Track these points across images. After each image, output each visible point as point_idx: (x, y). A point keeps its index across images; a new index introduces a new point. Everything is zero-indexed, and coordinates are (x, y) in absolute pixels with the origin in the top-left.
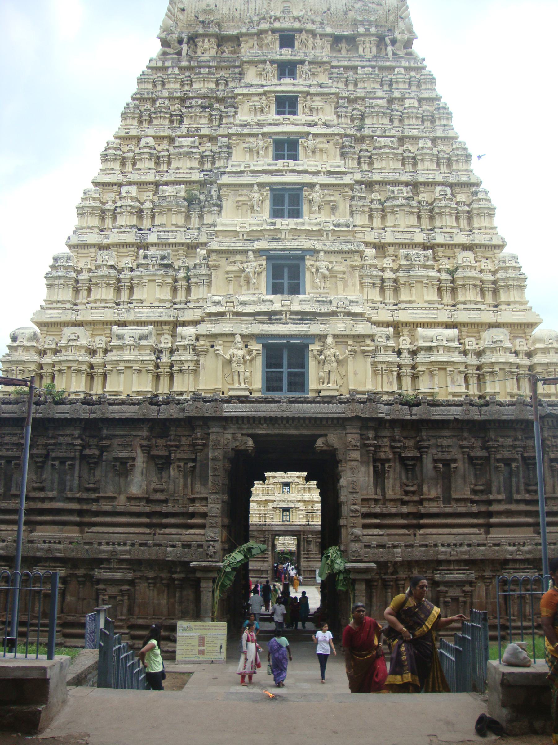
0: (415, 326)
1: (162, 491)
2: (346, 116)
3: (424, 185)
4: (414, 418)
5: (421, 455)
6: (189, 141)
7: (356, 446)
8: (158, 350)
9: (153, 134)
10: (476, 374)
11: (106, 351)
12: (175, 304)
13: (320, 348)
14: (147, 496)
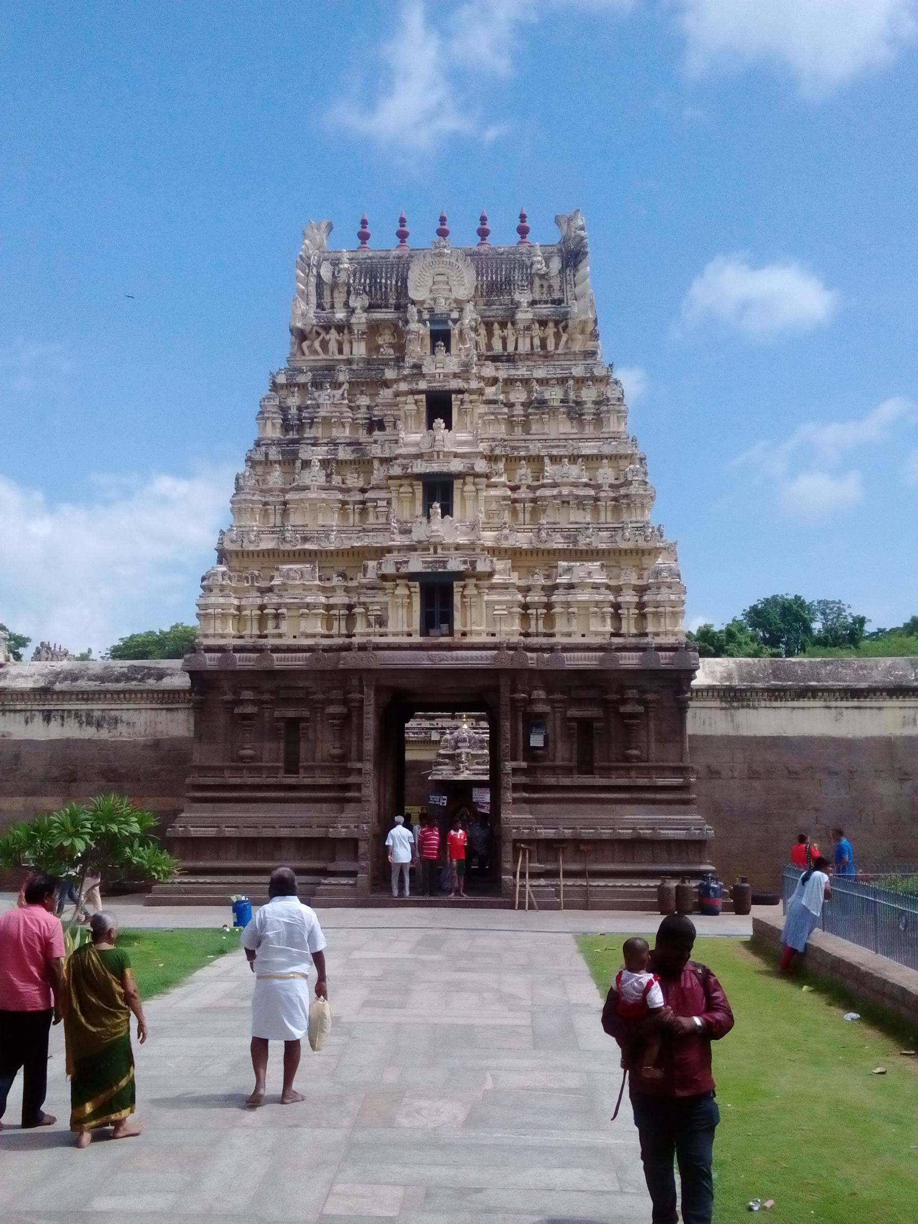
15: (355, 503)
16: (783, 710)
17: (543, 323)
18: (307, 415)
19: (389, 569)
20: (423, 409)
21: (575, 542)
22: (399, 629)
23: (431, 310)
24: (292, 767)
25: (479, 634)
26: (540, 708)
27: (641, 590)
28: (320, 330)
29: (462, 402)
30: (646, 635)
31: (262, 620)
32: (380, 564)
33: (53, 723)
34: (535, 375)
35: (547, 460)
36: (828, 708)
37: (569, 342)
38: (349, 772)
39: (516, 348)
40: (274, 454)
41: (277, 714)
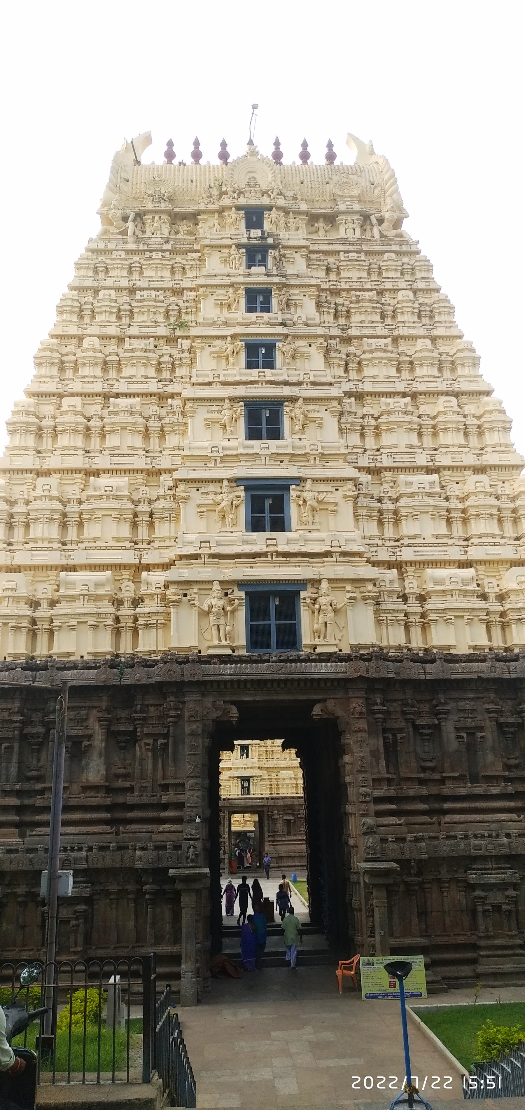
0: (422, 565)
1: (126, 776)
2: (328, 312)
3: (425, 395)
4: (428, 677)
5: (440, 723)
6: (142, 343)
7: (361, 713)
8: (117, 599)
9: (98, 333)
10: (499, 622)
11: (53, 603)
12: (136, 543)
13: (313, 595)
14: (108, 784)
26: (276, 816)
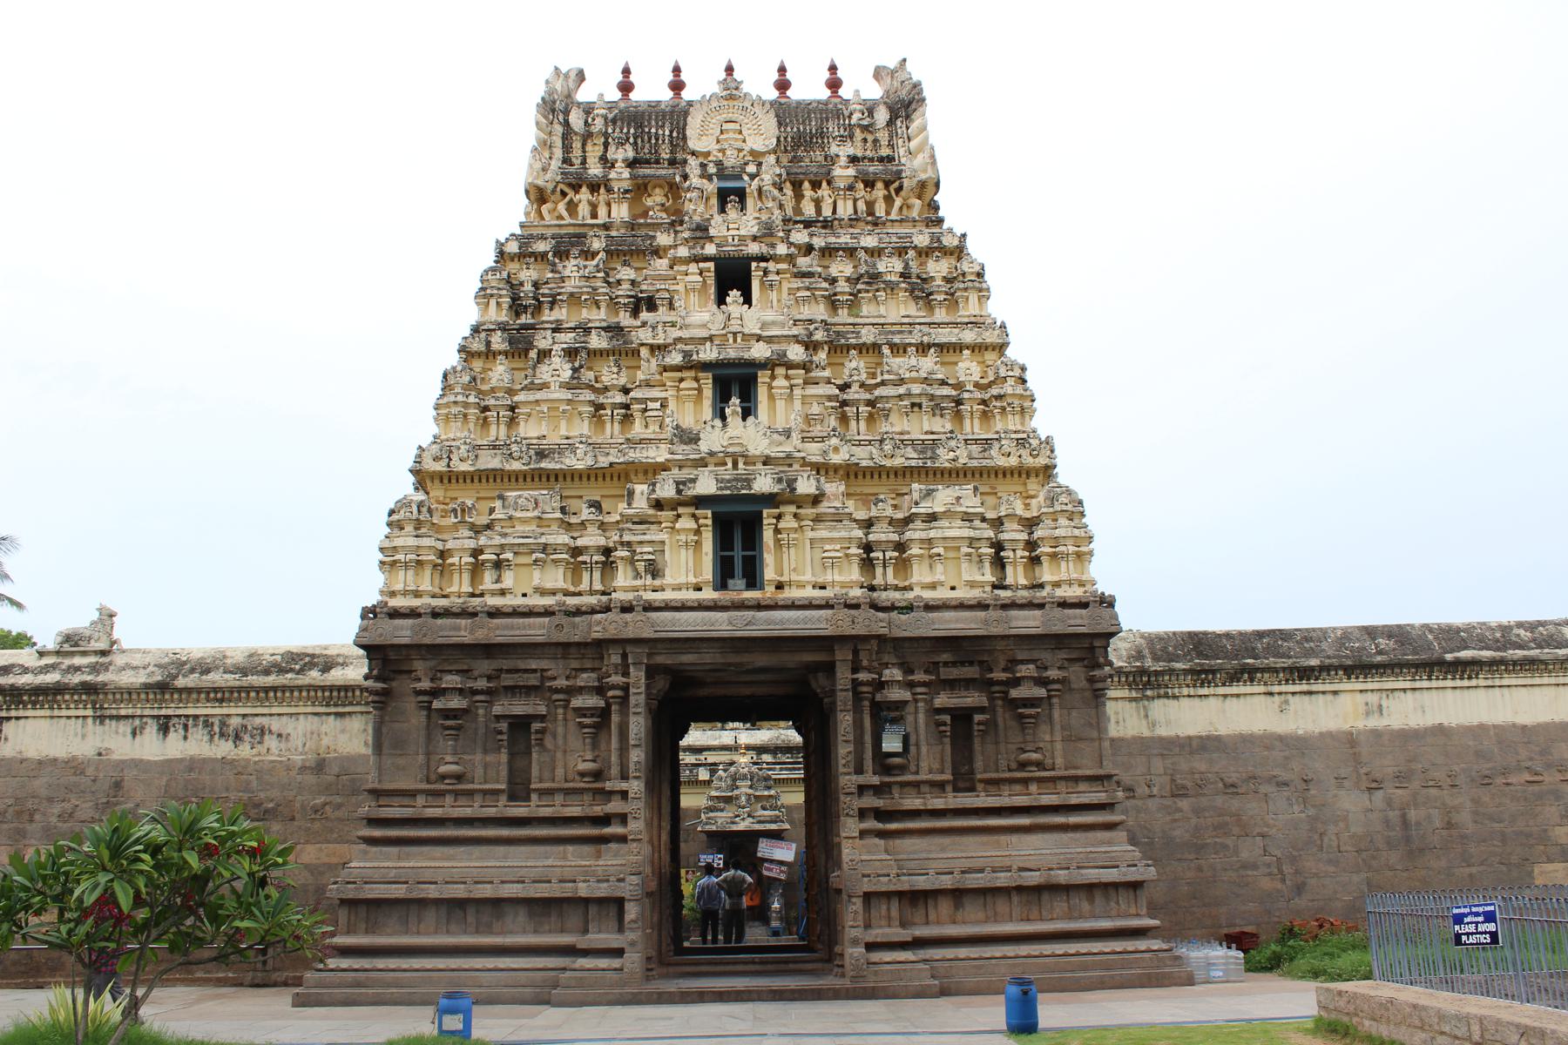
15: (615, 406)
16: (1211, 698)
17: (870, 184)
18: (547, 291)
19: (667, 491)
20: (711, 282)
21: (934, 458)
22: (682, 580)
23: (719, 164)
24: (519, 790)
25: (801, 586)
26: (896, 694)
27: (1031, 524)
28: (566, 189)
29: (766, 272)
30: (1041, 586)
31: (476, 570)
32: (654, 484)
33: (172, 735)
34: (863, 244)
35: (886, 350)
36: (1271, 694)
37: (905, 208)
38: (608, 795)
39: (834, 212)
40: (498, 342)
41: (497, 709)
